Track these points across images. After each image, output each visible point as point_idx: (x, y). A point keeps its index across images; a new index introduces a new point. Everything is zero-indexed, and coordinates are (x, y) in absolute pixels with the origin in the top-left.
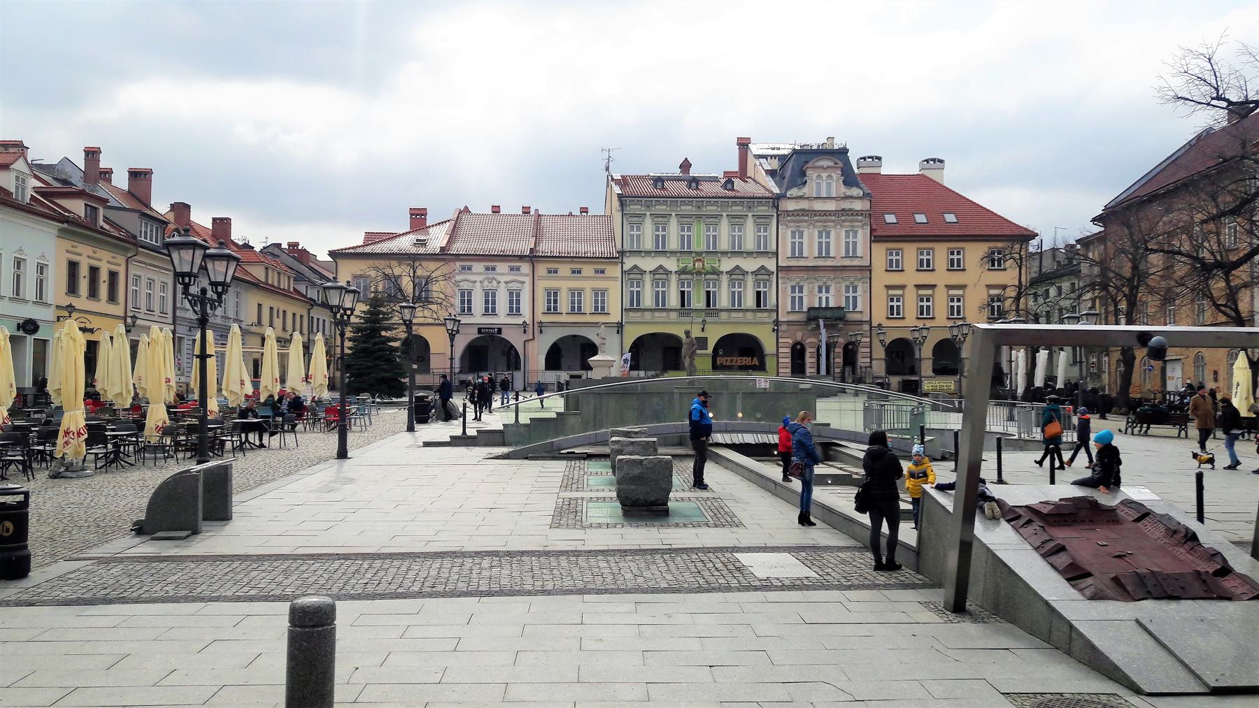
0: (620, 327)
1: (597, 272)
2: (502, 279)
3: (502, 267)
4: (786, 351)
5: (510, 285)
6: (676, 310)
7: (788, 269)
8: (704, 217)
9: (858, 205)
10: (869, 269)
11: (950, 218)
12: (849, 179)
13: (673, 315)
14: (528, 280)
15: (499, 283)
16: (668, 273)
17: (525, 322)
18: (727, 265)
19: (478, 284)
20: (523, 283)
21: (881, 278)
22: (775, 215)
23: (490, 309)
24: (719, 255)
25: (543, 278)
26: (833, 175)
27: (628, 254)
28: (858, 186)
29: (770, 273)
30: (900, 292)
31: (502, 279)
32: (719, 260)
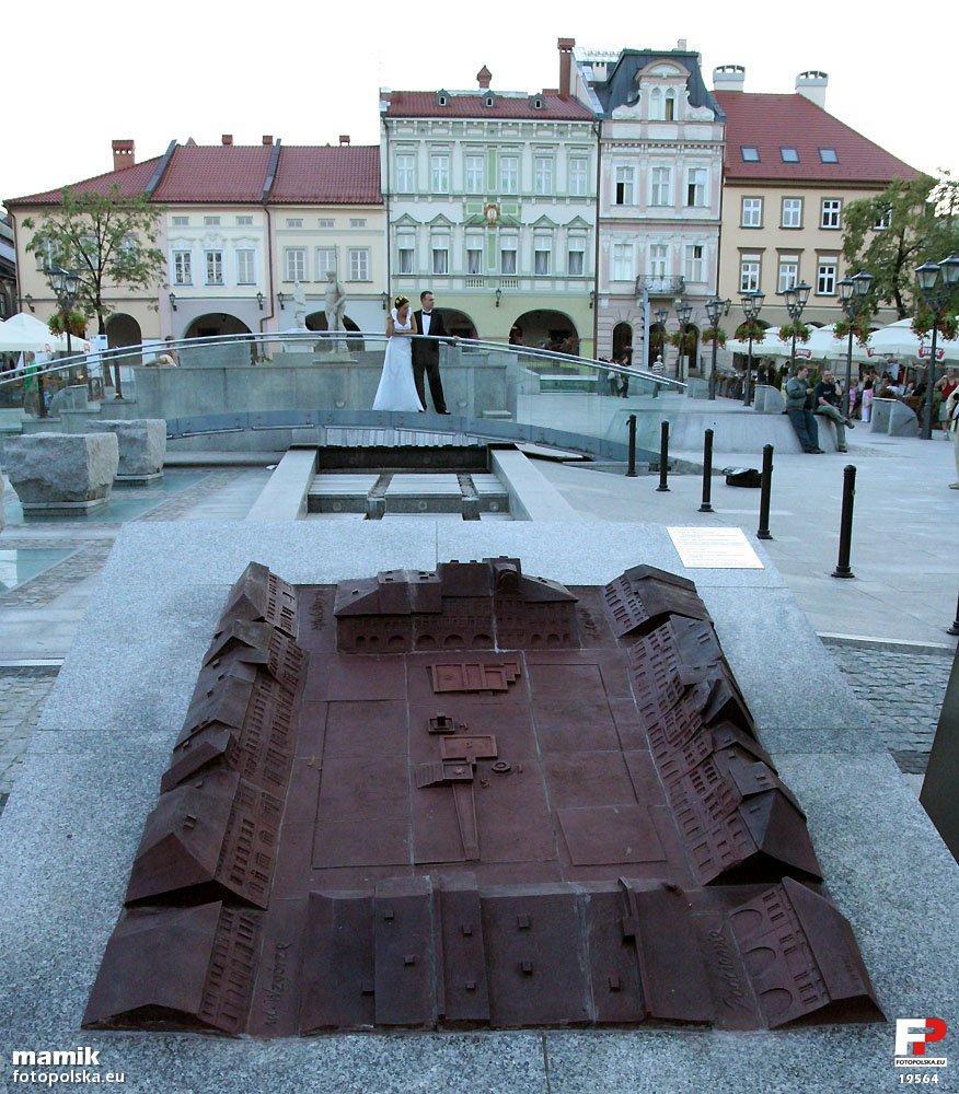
1: (354, 222)
2: (229, 235)
3: (228, 218)
4: (606, 336)
5: (239, 243)
6: (461, 277)
7: (613, 222)
8: (499, 147)
9: (706, 133)
11: (828, 156)
12: (697, 96)
13: (458, 285)
14: (262, 235)
15: (224, 240)
16: (450, 225)
17: (260, 294)
18: (530, 213)
19: (197, 244)
20: (256, 240)
21: (734, 238)
22: (596, 144)
23: (215, 278)
24: (520, 200)
26: (676, 88)
27: (396, 199)
28: (708, 106)
30: (757, 257)
31: (229, 235)
32: (520, 207)
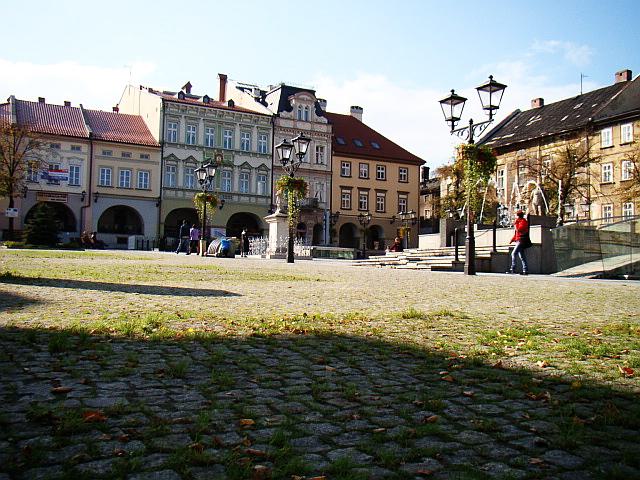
0: (159, 202)
9: (324, 129)
10: (331, 173)
14: (86, 158)
18: (239, 160)
20: (82, 160)
21: (338, 181)
25: (97, 157)
29: (267, 170)
30: (349, 191)
